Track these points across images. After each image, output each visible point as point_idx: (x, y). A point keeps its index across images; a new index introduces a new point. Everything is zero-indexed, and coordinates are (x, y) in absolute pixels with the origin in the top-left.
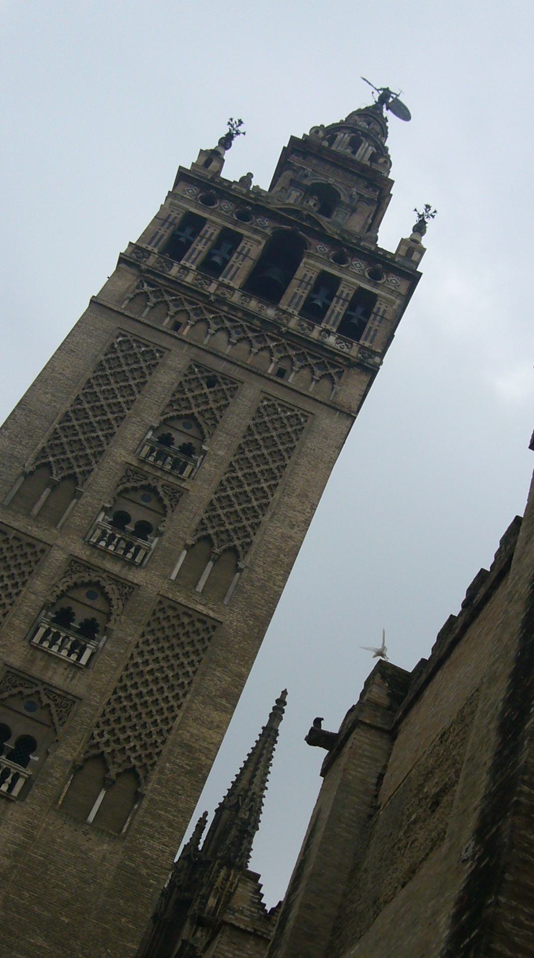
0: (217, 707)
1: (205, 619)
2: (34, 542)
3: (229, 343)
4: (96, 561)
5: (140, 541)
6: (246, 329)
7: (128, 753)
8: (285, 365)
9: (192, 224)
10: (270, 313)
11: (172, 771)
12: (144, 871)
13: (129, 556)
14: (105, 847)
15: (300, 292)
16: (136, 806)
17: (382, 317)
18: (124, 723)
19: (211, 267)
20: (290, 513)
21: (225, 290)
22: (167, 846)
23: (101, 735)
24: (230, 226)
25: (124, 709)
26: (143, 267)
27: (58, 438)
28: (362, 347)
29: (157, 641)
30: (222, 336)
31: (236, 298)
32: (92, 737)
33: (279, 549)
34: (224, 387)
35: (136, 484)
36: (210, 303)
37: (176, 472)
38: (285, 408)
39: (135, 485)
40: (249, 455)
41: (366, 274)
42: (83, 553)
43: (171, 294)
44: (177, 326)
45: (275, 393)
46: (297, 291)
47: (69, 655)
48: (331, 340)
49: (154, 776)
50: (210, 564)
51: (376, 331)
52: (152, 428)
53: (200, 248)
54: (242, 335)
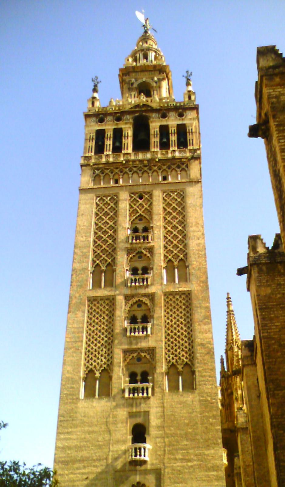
0: (205, 324)
1: (184, 292)
2: (108, 297)
3: (140, 177)
4: (134, 292)
5: (146, 276)
6: (143, 167)
7: (182, 358)
8: (164, 174)
9: (100, 135)
10: (149, 156)
11: (201, 356)
12: (209, 399)
13: (145, 283)
14: (191, 396)
15: (156, 140)
16: (194, 376)
17: (192, 132)
19: (117, 149)
20: (195, 234)
21: (126, 156)
22: (212, 385)
23: (169, 357)
24: (116, 127)
25: (172, 343)
26: (92, 164)
27: (96, 252)
28: (190, 150)
29: (171, 310)
30: (135, 175)
31: (133, 158)
32: (166, 359)
33: (198, 250)
34: (146, 196)
36: (124, 164)
37: (146, 241)
39: (133, 254)
41: (177, 117)
42: (128, 292)
43: (108, 169)
46: (155, 140)
47: (143, 333)
50: (176, 270)
51: (192, 139)
54: (143, 171)
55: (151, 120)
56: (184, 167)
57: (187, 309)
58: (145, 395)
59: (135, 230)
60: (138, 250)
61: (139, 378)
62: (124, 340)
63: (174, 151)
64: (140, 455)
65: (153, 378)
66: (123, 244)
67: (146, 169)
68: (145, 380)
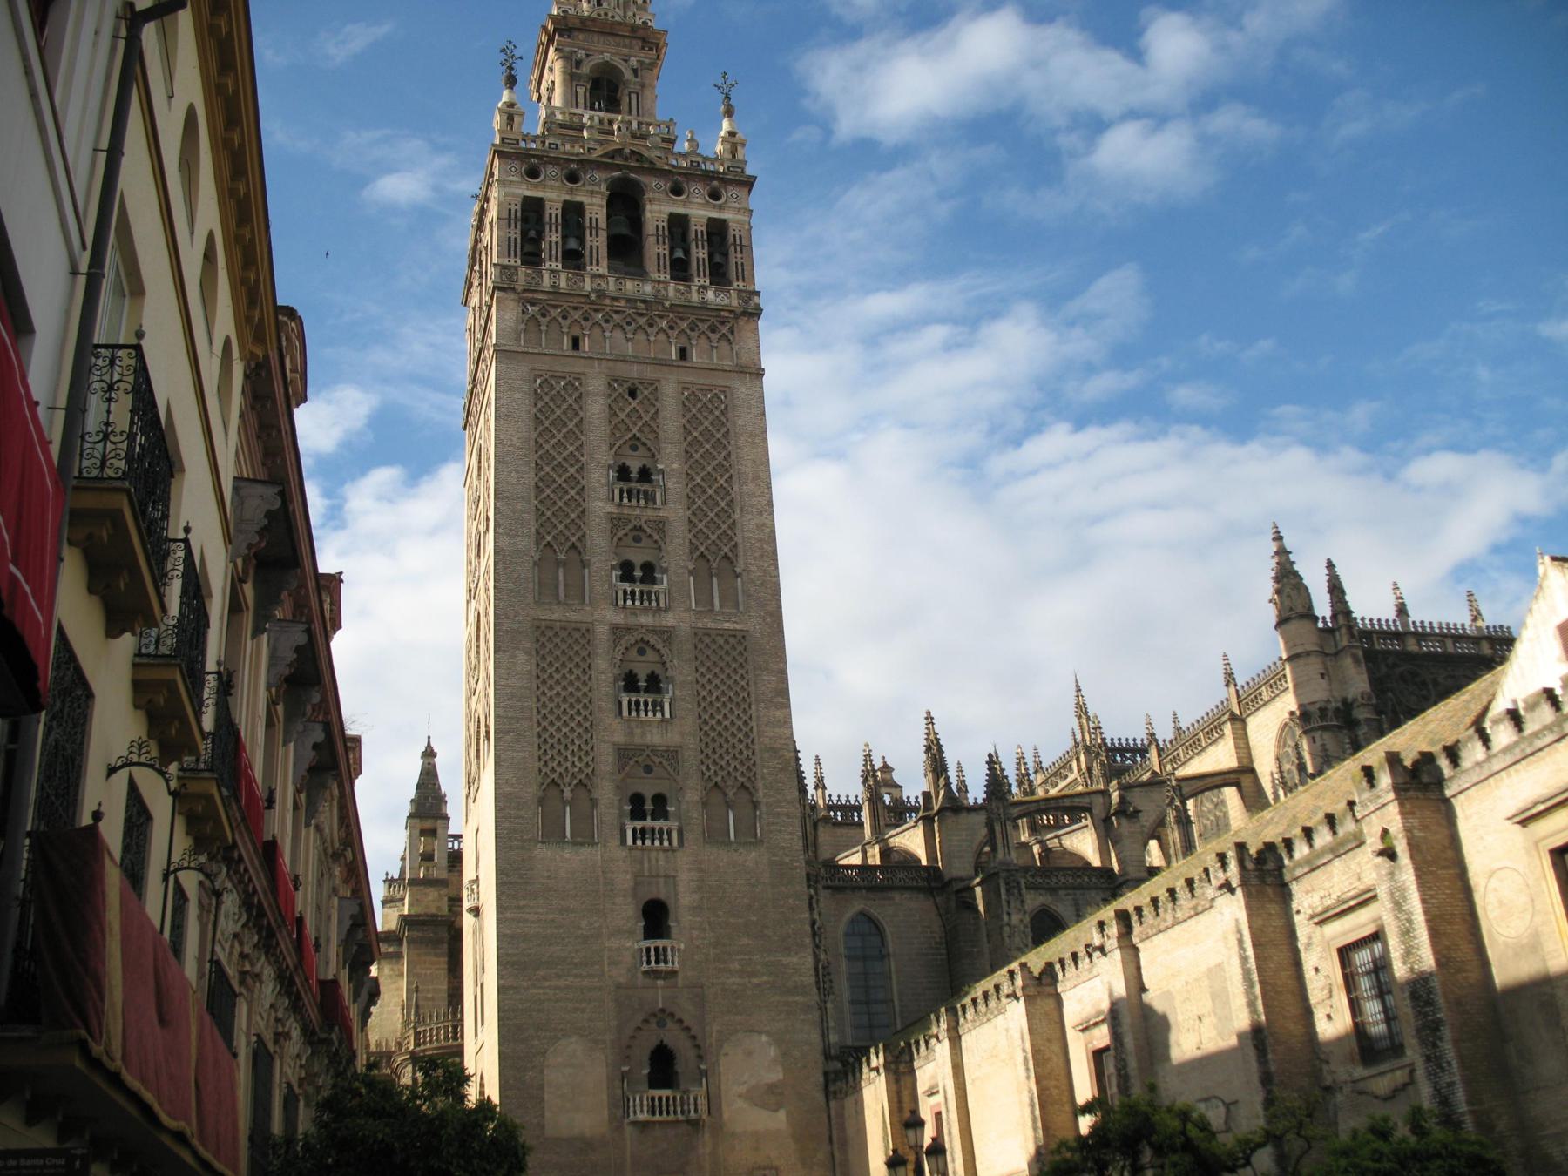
3: (628, 340)
4: (632, 621)
5: (656, 587)
8: (683, 341)
12: (787, 860)
18: (719, 751)
20: (754, 501)
21: (598, 281)
24: (568, 198)
30: (618, 334)
31: (611, 286)
33: (760, 540)
35: (627, 531)
36: (592, 302)
38: (704, 391)
40: (697, 456)
43: (555, 307)
44: (576, 343)
45: (689, 379)
48: (710, 295)
49: (760, 784)
50: (715, 580)
52: (610, 467)
53: (554, 239)
55: (649, 195)
56: (725, 330)
57: (741, 671)
58: (666, 843)
59: (623, 473)
60: (634, 522)
61: (649, 806)
62: (616, 724)
63: (704, 287)
64: (666, 962)
65: (679, 809)
66: (600, 504)
67: (642, 321)
68: (660, 811)
